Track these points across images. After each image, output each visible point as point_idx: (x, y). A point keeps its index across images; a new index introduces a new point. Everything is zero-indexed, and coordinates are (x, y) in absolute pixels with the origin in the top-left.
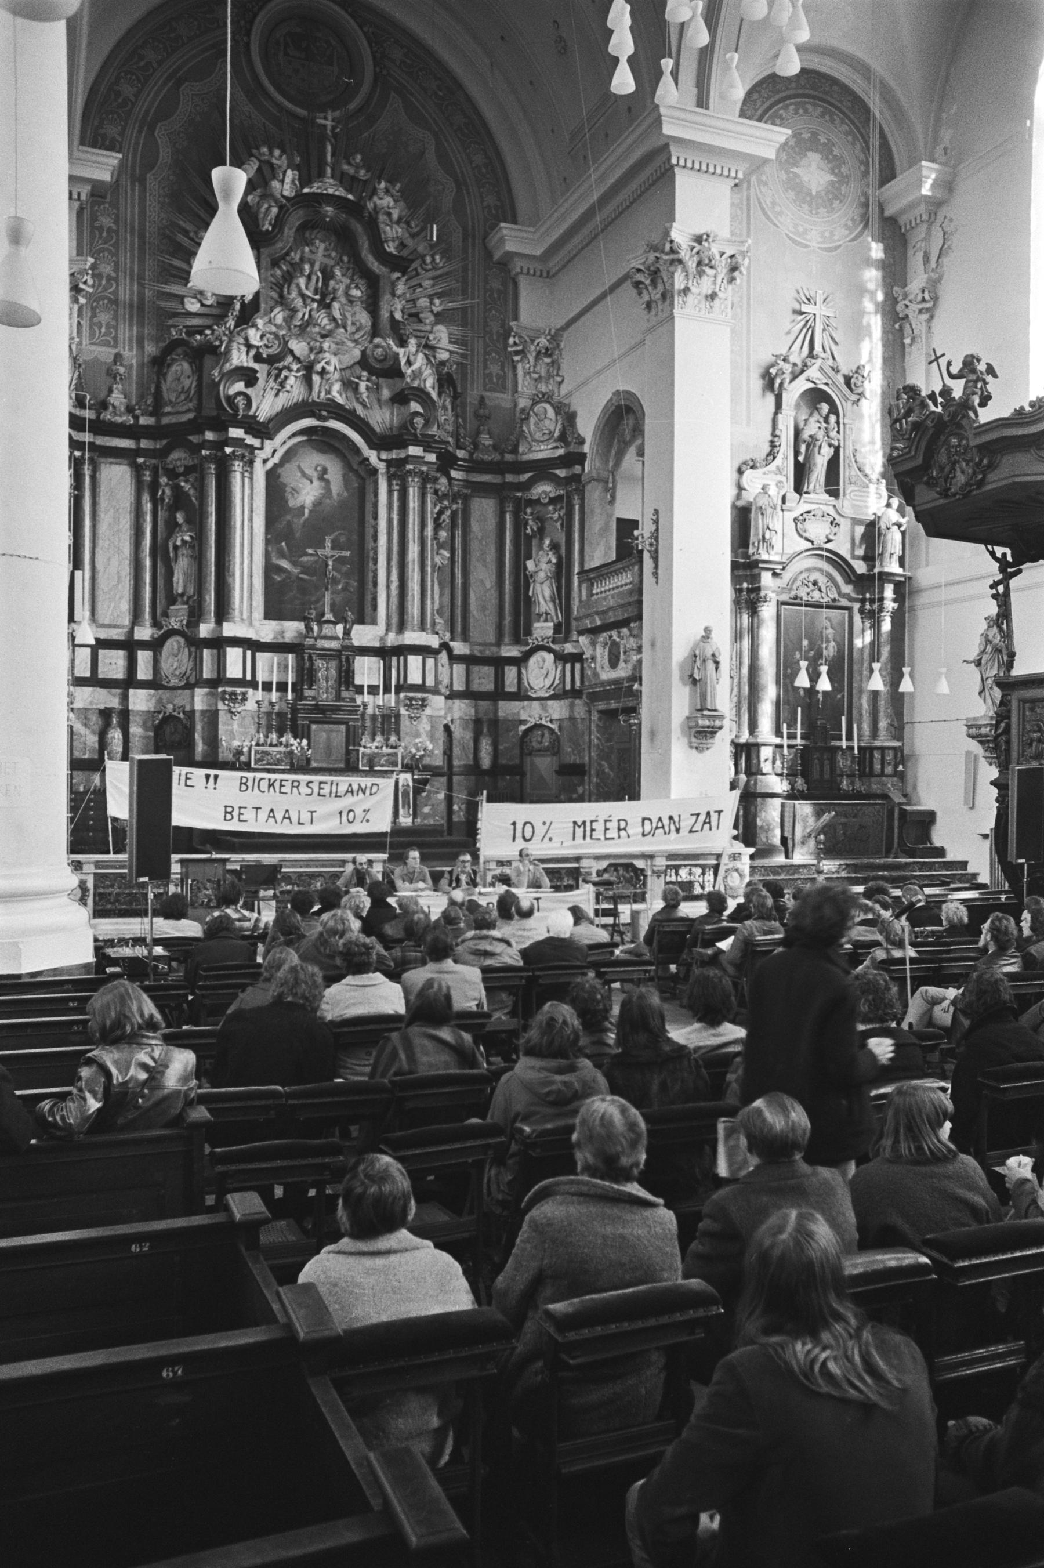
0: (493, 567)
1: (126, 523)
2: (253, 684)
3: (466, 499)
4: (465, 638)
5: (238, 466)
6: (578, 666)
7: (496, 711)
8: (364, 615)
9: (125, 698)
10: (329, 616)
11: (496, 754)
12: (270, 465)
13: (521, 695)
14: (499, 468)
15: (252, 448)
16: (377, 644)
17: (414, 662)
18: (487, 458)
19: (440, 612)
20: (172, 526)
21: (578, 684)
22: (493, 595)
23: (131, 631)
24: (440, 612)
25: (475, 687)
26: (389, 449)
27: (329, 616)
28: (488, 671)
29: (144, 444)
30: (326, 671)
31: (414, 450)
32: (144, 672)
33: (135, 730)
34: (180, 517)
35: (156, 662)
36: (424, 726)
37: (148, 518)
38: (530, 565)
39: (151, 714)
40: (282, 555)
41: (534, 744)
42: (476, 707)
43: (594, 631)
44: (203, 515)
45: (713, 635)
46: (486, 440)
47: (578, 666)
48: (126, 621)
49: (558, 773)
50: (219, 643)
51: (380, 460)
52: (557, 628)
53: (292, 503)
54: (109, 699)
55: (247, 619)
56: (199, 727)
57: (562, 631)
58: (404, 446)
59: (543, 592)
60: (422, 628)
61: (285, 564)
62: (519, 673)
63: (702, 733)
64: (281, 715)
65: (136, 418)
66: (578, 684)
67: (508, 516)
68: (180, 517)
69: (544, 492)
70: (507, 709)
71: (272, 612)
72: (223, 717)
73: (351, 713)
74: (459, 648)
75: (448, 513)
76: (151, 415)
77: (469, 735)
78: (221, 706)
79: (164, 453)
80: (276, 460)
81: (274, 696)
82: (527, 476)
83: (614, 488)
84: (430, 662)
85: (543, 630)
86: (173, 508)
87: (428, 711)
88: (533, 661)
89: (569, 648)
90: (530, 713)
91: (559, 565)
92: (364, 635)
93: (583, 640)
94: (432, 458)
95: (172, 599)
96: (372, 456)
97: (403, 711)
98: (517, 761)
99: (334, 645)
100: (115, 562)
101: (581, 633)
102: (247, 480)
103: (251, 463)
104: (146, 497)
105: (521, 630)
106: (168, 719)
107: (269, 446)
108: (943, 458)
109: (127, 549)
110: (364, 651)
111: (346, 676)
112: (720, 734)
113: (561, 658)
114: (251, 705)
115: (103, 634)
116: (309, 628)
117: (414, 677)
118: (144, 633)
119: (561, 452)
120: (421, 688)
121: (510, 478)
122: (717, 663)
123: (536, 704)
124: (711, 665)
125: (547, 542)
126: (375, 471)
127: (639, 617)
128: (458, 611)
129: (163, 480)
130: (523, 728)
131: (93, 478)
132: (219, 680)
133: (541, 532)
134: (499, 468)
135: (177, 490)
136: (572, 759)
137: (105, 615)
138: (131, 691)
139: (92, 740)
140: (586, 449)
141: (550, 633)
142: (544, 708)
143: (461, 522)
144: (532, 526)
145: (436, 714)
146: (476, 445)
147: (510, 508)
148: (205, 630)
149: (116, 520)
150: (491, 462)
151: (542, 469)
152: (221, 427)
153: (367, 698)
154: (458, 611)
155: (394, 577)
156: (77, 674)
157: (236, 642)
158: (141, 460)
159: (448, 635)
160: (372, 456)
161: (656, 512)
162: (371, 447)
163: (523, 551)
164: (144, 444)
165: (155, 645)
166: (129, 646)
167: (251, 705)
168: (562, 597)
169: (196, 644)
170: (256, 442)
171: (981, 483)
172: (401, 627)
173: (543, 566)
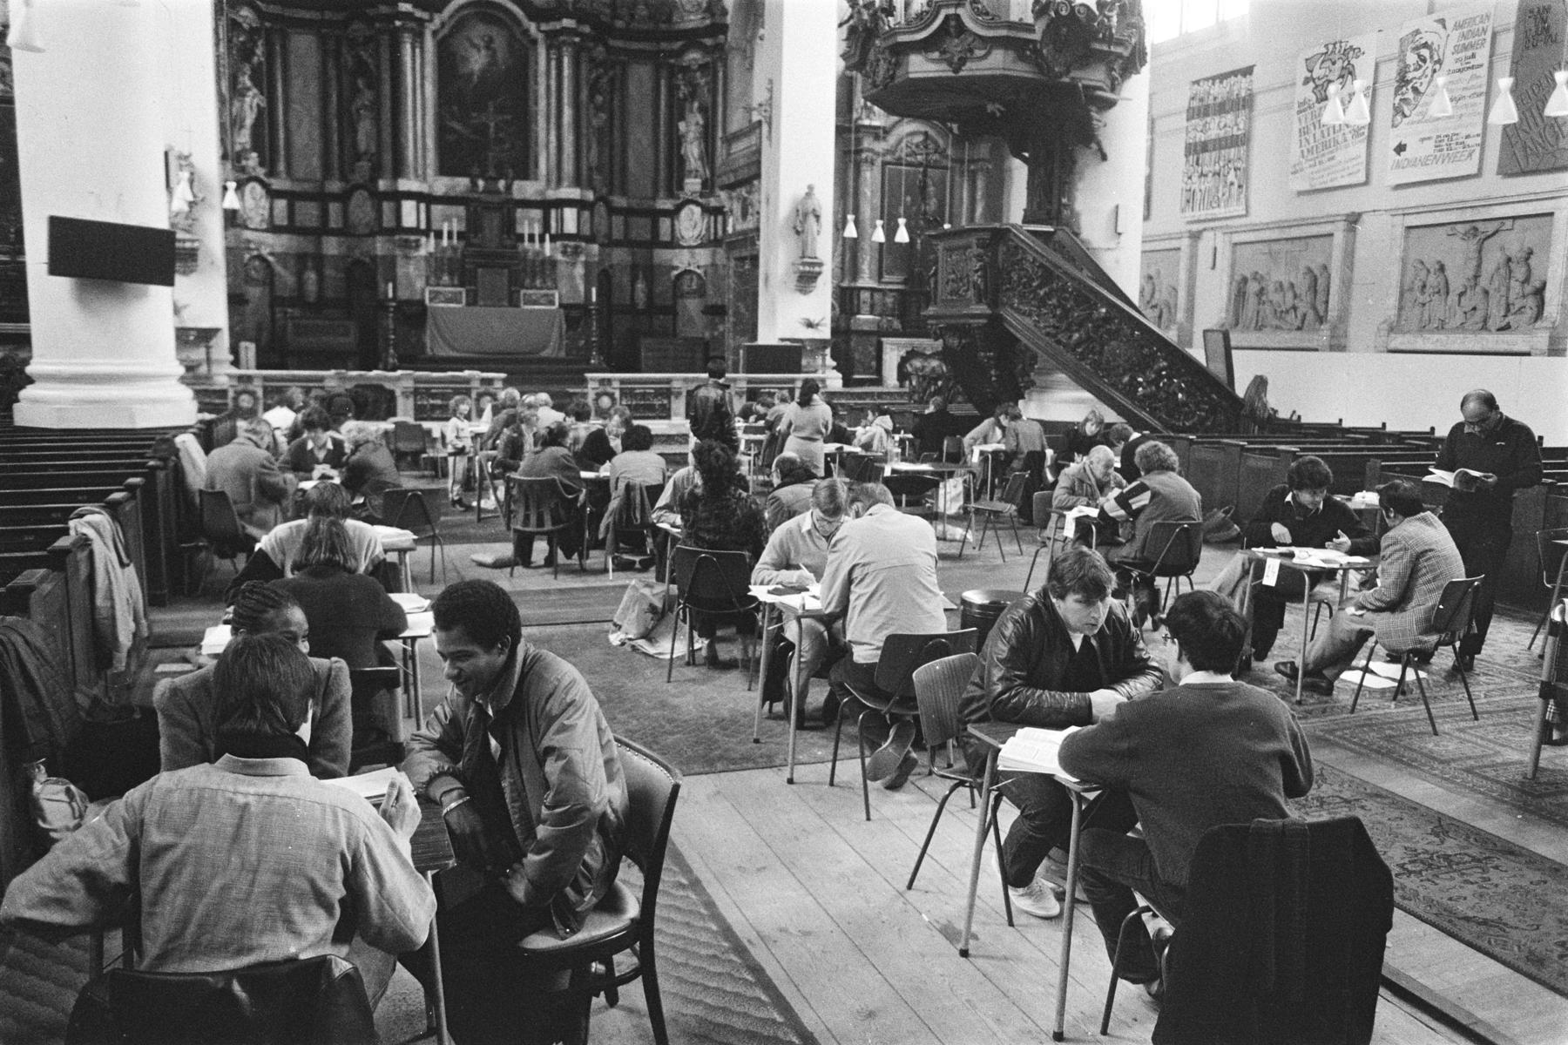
1: (314, 88)
2: (426, 233)
3: (624, 67)
4: (624, 193)
6: (720, 218)
7: (652, 258)
8: (525, 170)
9: (319, 244)
10: (492, 173)
11: (650, 294)
12: (440, 35)
13: (674, 244)
15: (421, 22)
17: (570, 214)
19: (599, 169)
20: (356, 91)
21: (720, 233)
22: (649, 153)
23: (322, 184)
24: (599, 169)
25: (633, 235)
26: (547, 20)
27: (492, 173)
28: (645, 222)
29: (328, 15)
30: (492, 222)
31: (568, 23)
32: (335, 221)
34: (360, 83)
36: (579, 270)
37: (334, 83)
38: (682, 126)
39: (342, 257)
41: (685, 288)
42: (633, 254)
43: (731, 187)
44: (379, 79)
45: (816, 191)
46: (642, 11)
47: (720, 218)
48: (319, 175)
49: (703, 312)
50: (398, 197)
52: (704, 184)
55: (422, 173)
56: (380, 269)
57: (708, 186)
58: (559, 19)
59: (692, 150)
60: (577, 182)
61: (457, 126)
62: (673, 225)
63: (806, 279)
66: (720, 233)
67: (663, 82)
68: (360, 83)
70: (662, 255)
71: (445, 169)
72: (400, 262)
73: (511, 258)
74: (619, 201)
75: (605, 80)
77: (626, 280)
78: (398, 252)
79: (345, 24)
80: (445, 31)
81: (445, 242)
82: (679, 44)
83: (752, 56)
84: (586, 214)
85: (693, 185)
87: (582, 258)
88: (684, 213)
89: (713, 202)
90: (681, 260)
91: (706, 126)
92: (526, 189)
93: (723, 195)
94: (587, 29)
95: (358, 157)
96: (532, 27)
97: (559, 257)
98: (669, 303)
99: (496, 199)
100: (305, 125)
101: (723, 188)
105: (674, 183)
106: (357, 262)
107: (438, 20)
108: (871, 56)
109: (315, 112)
110: (527, 204)
111: (509, 225)
112: (820, 279)
113: (707, 210)
114: (422, 252)
115: (297, 188)
116: (474, 184)
117: (570, 227)
118: (335, 186)
119: (708, 22)
122: (817, 217)
123: (685, 251)
124: (812, 219)
125: (696, 105)
126: (534, 42)
127: (758, 176)
129: (344, 50)
130: (675, 273)
131: (284, 47)
132: (399, 228)
133: (693, 95)
136: (713, 300)
137: (300, 173)
138: (325, 239)
140: (729, 19)
141: (698, 188)
142: (693, 256)
143: (619, 86)
144: (683, 90)
146: (632, 16)
147: (664, 73)
148: (382, 185)
150: (647, 32)
151: (692, 38)
153: (526, 244)
155: (553, 138)
156: (278, 222)
157: (410, 195)
159: (604, 191)
160: (532, 27)
161: (771, 81)
162: (531, 19)
163: (677, 112)
164: (328, 15)
165: (344, 198)
166: (322, 198)
168: (708, 155)
169: (378, 197)
170: (425, 16)
171: (892, 77)
173: (693, 128)
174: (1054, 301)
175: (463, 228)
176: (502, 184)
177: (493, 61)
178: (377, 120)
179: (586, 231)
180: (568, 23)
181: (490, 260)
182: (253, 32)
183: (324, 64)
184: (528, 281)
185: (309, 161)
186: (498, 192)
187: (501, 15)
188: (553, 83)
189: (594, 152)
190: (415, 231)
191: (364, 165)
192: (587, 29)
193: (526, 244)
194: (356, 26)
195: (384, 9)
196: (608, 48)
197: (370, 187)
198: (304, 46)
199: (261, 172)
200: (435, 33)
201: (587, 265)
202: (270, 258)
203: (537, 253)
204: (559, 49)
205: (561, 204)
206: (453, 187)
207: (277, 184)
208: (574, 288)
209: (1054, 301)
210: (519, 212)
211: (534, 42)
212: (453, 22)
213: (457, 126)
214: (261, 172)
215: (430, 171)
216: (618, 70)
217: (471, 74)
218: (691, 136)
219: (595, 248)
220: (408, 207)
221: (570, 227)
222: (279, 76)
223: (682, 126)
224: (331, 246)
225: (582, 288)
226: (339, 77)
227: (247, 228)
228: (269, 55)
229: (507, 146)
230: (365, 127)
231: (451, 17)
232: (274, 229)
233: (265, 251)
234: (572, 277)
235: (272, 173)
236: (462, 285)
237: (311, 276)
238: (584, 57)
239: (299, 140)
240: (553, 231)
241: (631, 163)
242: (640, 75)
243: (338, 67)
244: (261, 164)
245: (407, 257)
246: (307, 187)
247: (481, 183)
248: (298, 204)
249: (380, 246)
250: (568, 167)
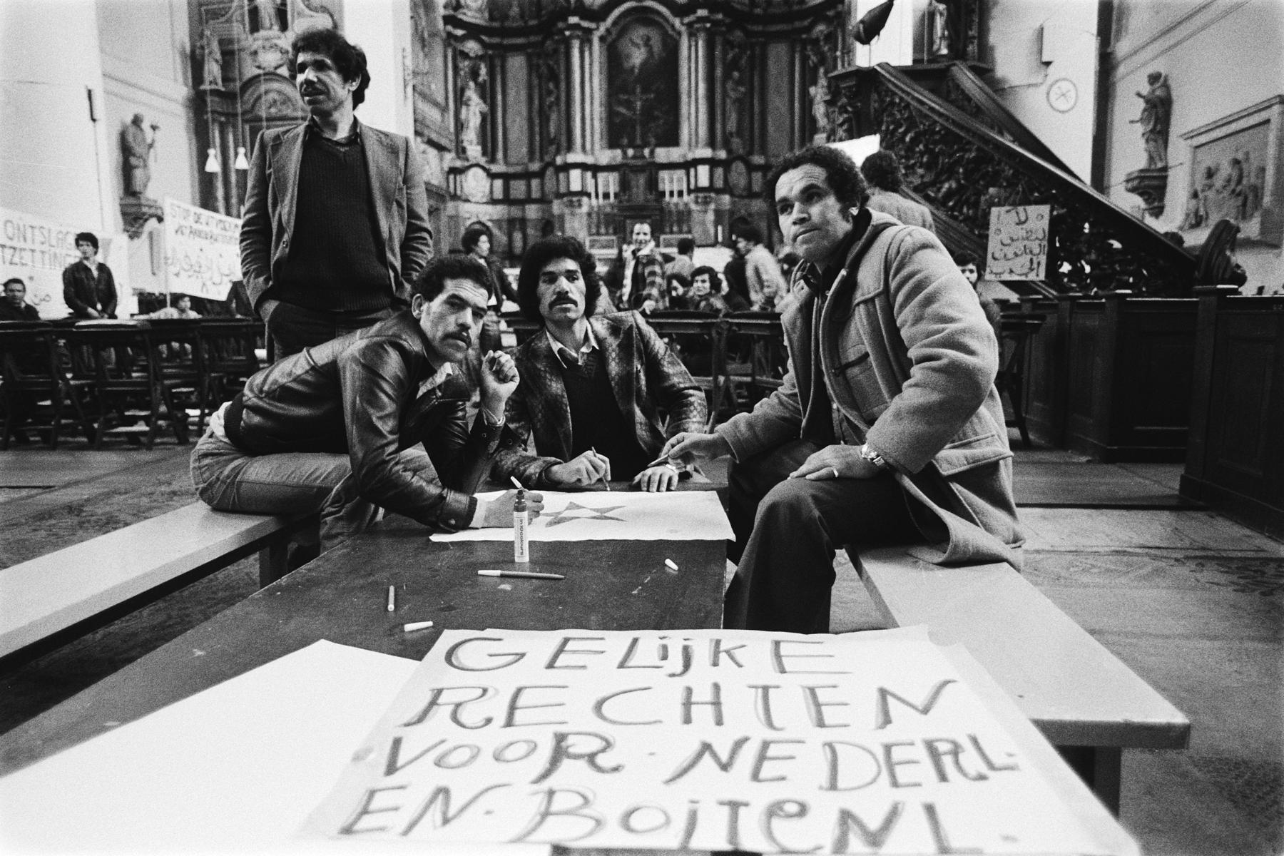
0: (786, 98)
2: (589, 195)
3: (764, 47)
4: (763, 151)
5: (576, 44)
8: (672, 139)
9: (524, 210)
10: (638, 142)
12: (609, 39)
14: (789, 17)
15: (589, 32)
16: (681, 160)
17: (703, 171)
18: (777, 11)
19: (739, 133)
20: (550, 93)
26: (687, 15)
27: (638, 142)
29: (533, 39)
31: (702, 12)
32: (535, 194)
33: (530, 231)
35: (542, 185)
36: (711, 217)
38: (812, 90)
40: (620, 103)
48: (526, 160)
50: (567, 167)
51: (682, 24)
53: (627, 65)
54: (515, 212)
60: (712, 143)
61: (623, 110)
64: (607, 215)
65: (526, 22)
68: (551, 86)
69: (821, 32)
71: (612, 143)
72: (568, 218)
74: (758, 159)
76: (534, 18)
79: (542, 43)
80: (614, 36)
84: (719, 171)
86: (549, 80)
87: (712, 206)
94: (720, 16)
95: (551, 142)
96: (677, 22)
97: (693, 207)
102: (587, 54)
103: (590, 42)
104: (534, 75)
111: (653, 184)
115: (511, 170)
116: (625, 153)
117: (704, 181)
118: (535, 166)
120: (711, 188)
121: (797, 24)
126: (679, 34)
128: (757, 131)
134: (789, 17)
135: (549, 67)
137: (512, 160)
139: (504, 239)
143: (759, 64)
145: (723, 208)
149: (518, 93)
152: (566, 20)
154: (757, 131)
158: (529, 51)
160: (677, 22)
162: (676, 15)
164: (533, 39)
165: (540, 174)
166: (527, 176)
167: (585, 209)
170: (593, 25)
172: (697, 145)
174: (921, 147)
175: (617, 189)
176: (646, 152)
177: (650, 52)
178: (559, 111)
179: (719, 183)
180: (702, 12)
181: (639, 214)
182: (481, 58)
183: (530, 74)
184: (668, 230)
185: (519, 150)
186: (644, 157)
187: (657, 18)
188: (693, 65)
189: (734, 116)
190: (584, 193)
191: (553, 148)
192: (720, 16)
193: (667, 198)
194: (548, 42)
195: (561, 25)
196: (748, 34)
197: (552, 163)
198: (517, 64)
199: (482, 161)
200: (602, 39)
201: (718, 213)
202: (490, 224)
203: (676, 205)
204: (695, 35)
205: (696, 162)
206: (614, 158)
207: (495, 168)
208: (706, 231)
209: (921, 147)
210: (664, 175)
211: (679, 34)
212: (619, 27)
213: (623, 110)
214: (482, 161)
215: (597, 146)
216: (758, 50)
217: (634, 67)
218: (818, 98)
219: (726, 198)
220: (575, 174)
221: (704, 181)
222: (499, 89)
223: (812, 90)
224: (532, 212)
225: (712, 231)
226: (540, 85)
227: (467, 201)
228: (491, 73)
229: (661, 122)
230: (554, 117)
231: (615, 23)
232: (493, 202)
233: (484, 219)
234: (703, 223)
235: (493, 160)
236: (615, 233)
237: (518, 236)
238: (719, 40)
239: (513, 136)
240: (692, 187)
241: (771, 129)
242: (778, 55)
243: (540, 77)
244: (484, 154)
245: (573, 214)
246: (519, 169)
247: (630, 152)
248: (512, 182)
249: (557, 207)
250: (703, 131)
